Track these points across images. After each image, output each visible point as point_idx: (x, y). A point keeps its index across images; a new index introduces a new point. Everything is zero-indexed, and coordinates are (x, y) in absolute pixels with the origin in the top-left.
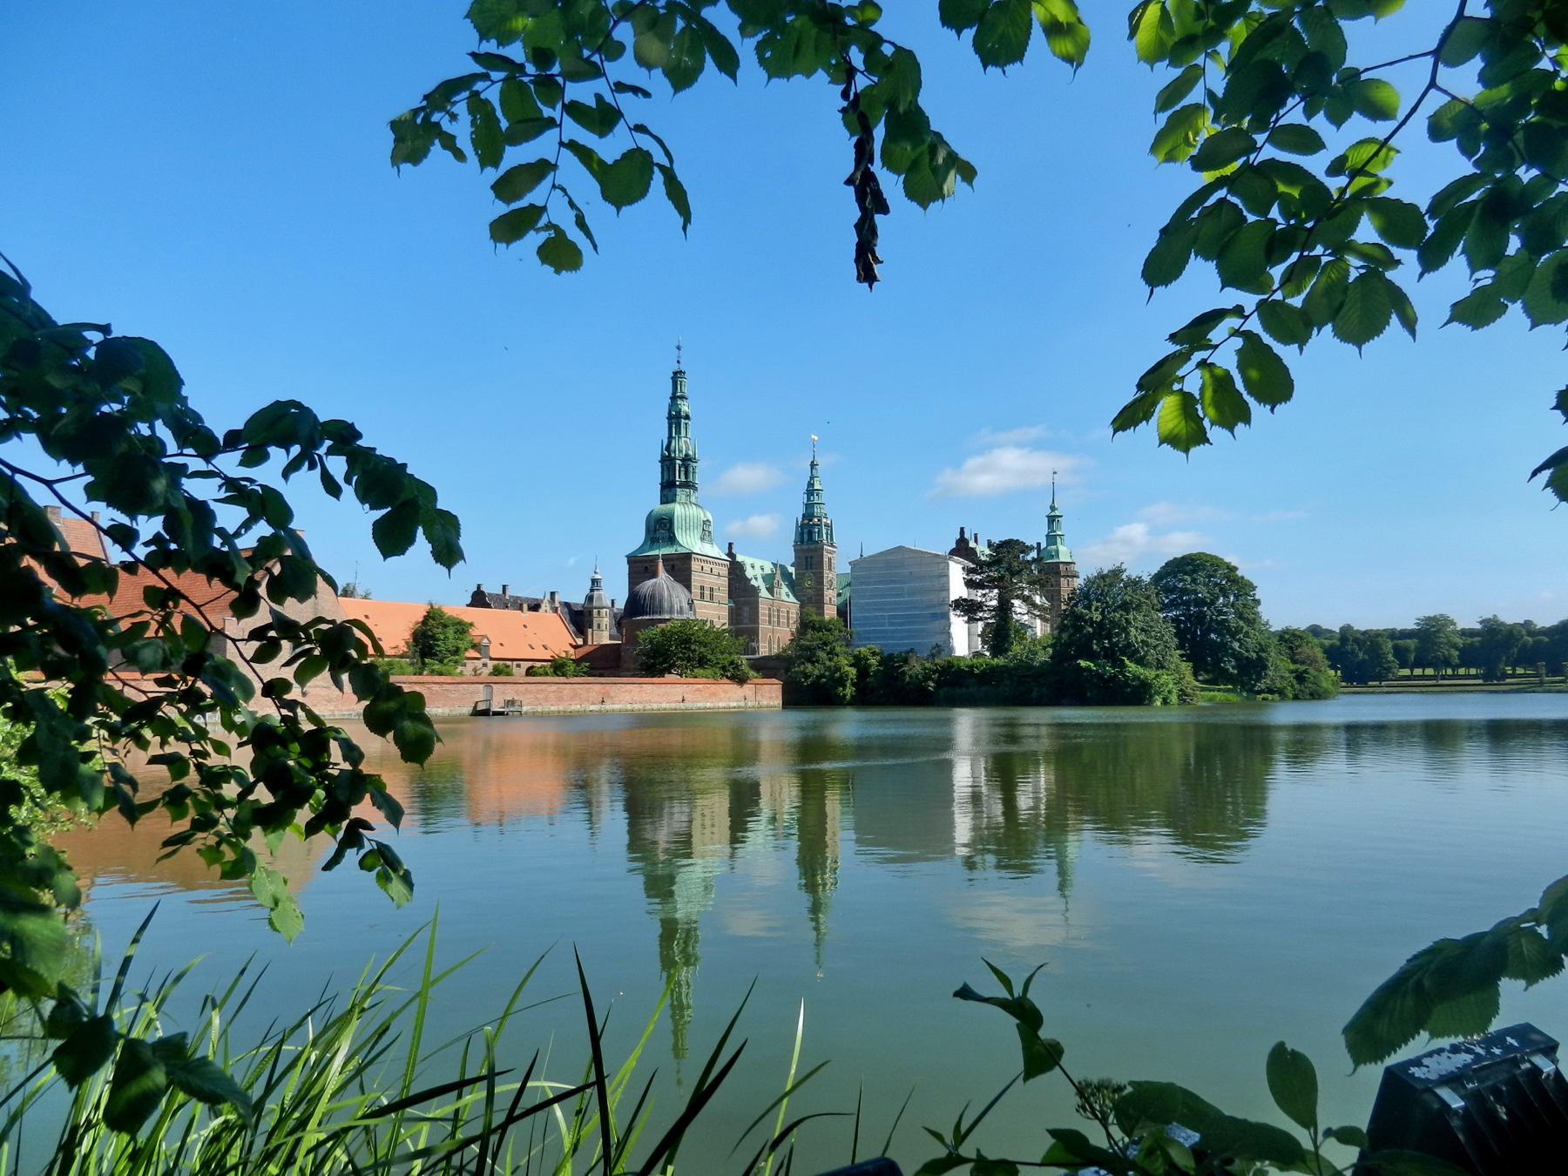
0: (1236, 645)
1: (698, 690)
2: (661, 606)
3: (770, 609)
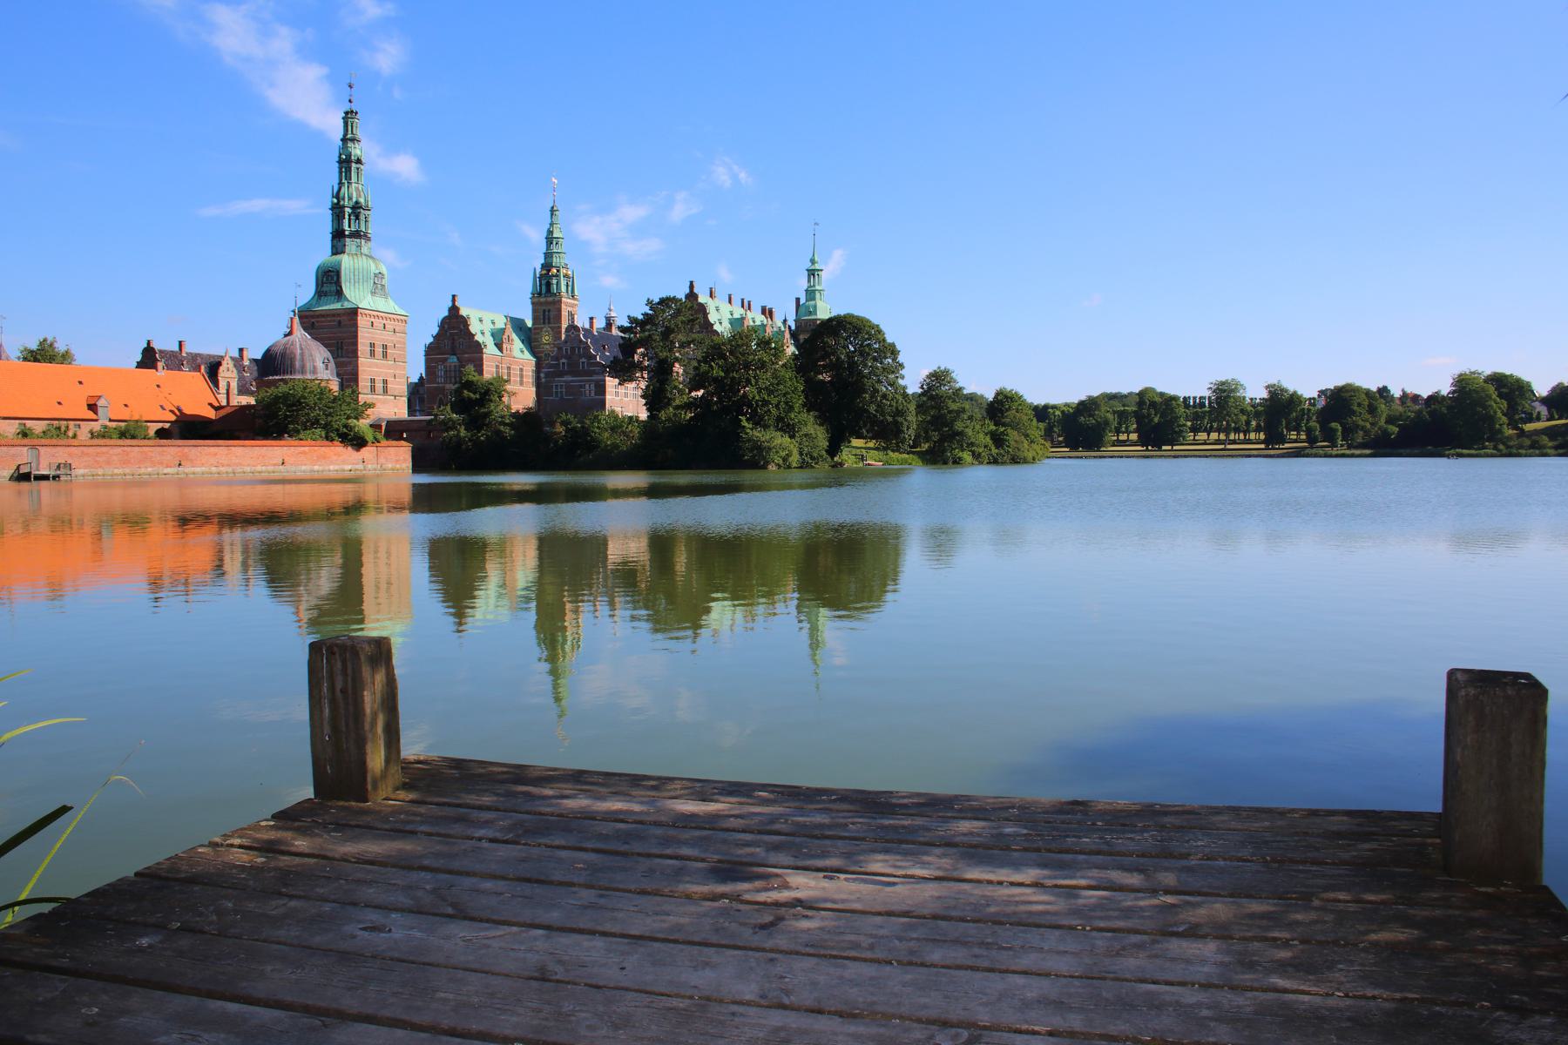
0: (872, 408)
1: (304, 453)
2: (292, 365)
3: (497, 367)
